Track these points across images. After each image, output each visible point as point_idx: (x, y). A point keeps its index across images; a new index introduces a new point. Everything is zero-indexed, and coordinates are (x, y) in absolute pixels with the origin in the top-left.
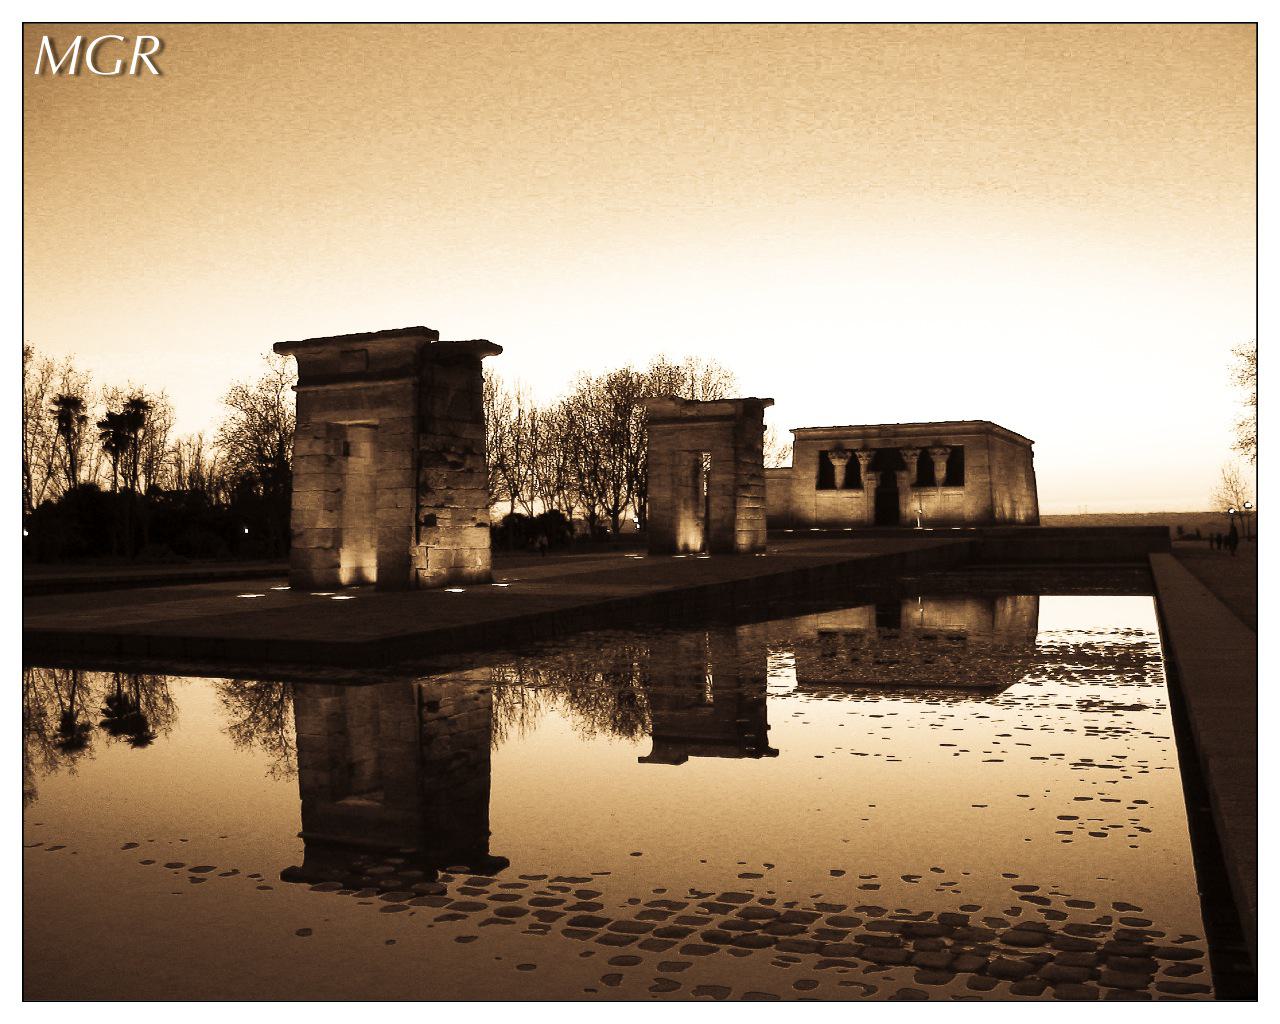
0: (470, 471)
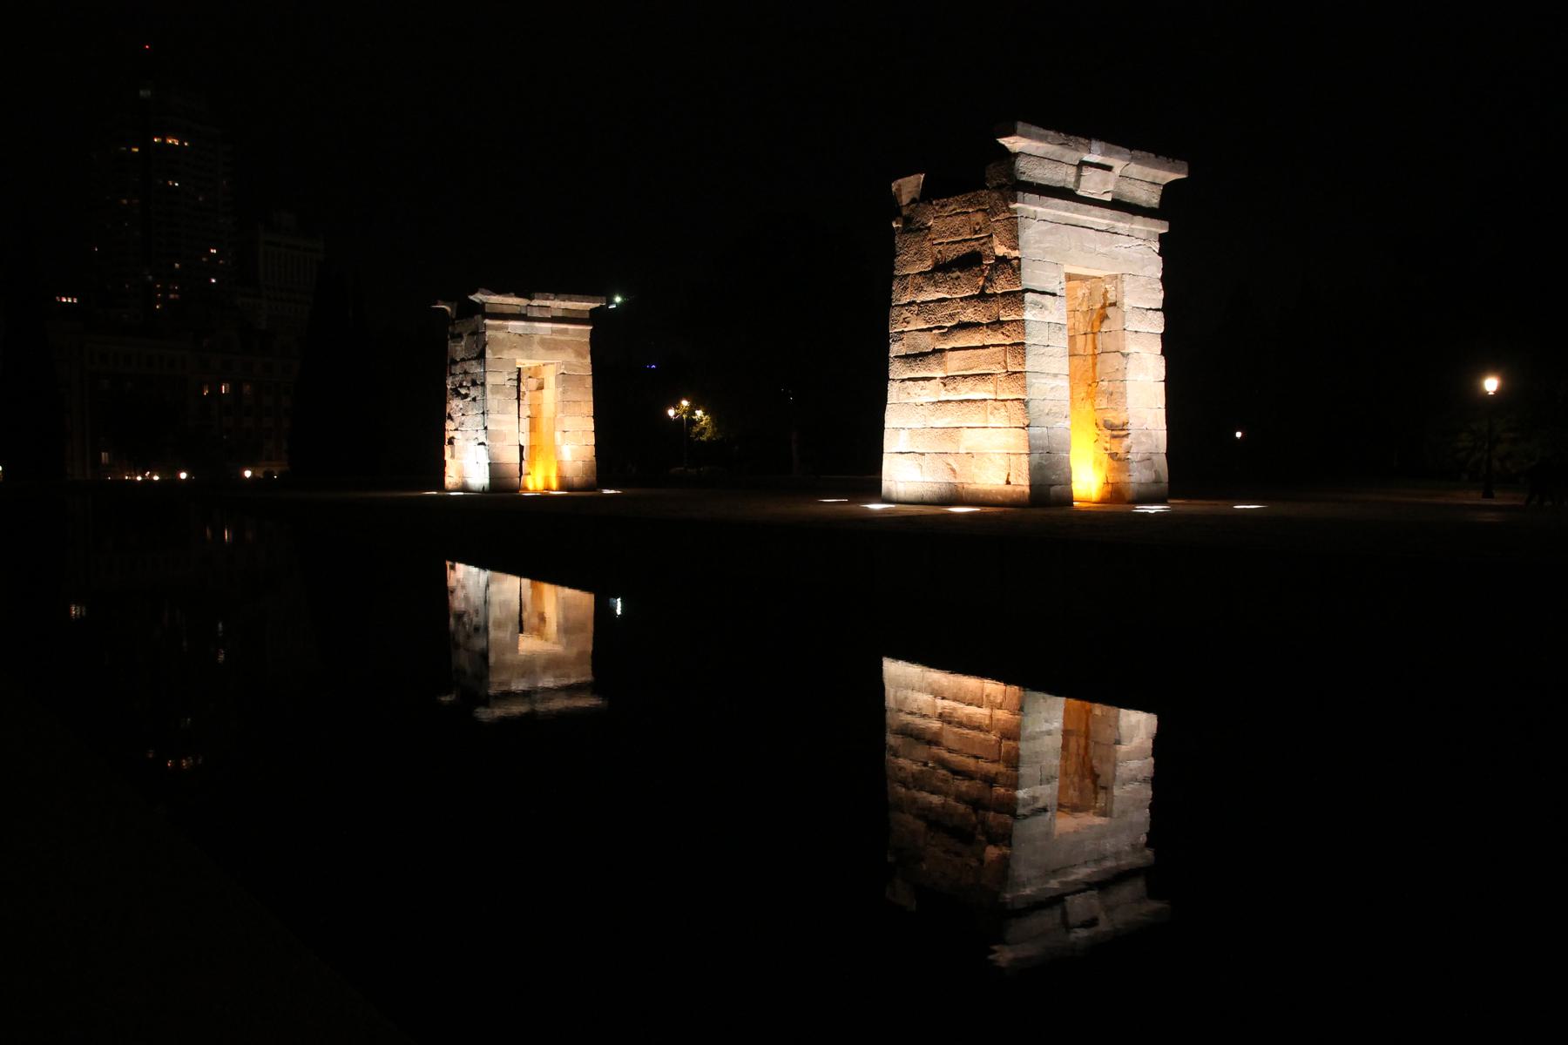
0: (474, 399)
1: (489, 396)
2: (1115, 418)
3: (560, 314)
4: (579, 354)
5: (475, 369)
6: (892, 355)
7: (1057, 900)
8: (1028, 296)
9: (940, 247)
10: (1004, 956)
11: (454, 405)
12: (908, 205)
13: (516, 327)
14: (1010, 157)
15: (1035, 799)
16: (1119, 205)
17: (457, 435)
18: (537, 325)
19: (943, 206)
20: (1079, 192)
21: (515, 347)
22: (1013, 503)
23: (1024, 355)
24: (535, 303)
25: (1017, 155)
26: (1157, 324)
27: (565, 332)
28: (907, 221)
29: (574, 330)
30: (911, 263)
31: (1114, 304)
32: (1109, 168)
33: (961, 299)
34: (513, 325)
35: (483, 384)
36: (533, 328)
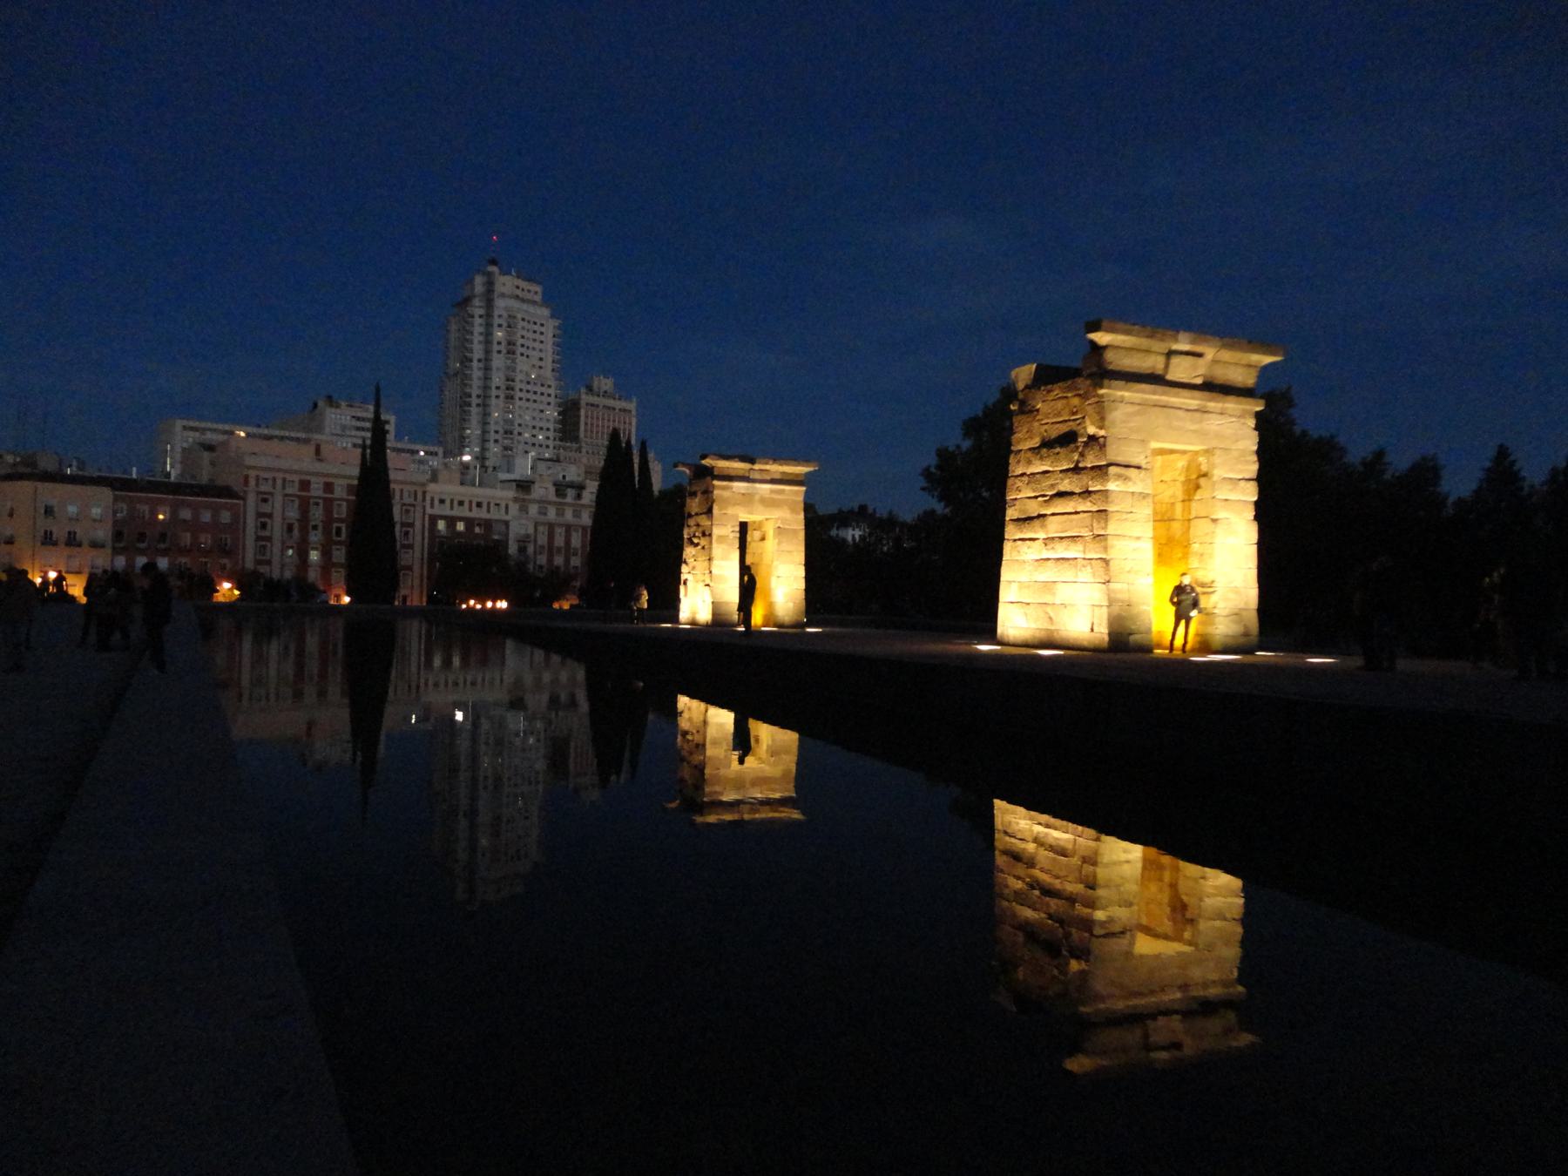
1: (715, 545)
4: (793, 511)
5: (704, 521)
6: (1007, 519)
8: (1112, 470)
9: (1046, 427)
10: (1078, 1064)
11: (689, 552)
12: (1023, 390)
13: (739, 488)
15: (1111, 920)
16: (1211, 387)
17: (689, 577)
18: (758, 485)
19: (1049, 391)
20: (1169, 377)
21: (738, 504)
22: (1096, 650)
23: (1106, 521)
24: (757, 467)
25: (1105, 347)
26: (1251, 493)
27: (782, 492)
28: (1023, 403)
29: (791, 491)
30: (1025, 439)
31: (1205, 475)
32: (1200, 355)
33: (1061, 471)
35: (710, 535)
36: (755, 488)
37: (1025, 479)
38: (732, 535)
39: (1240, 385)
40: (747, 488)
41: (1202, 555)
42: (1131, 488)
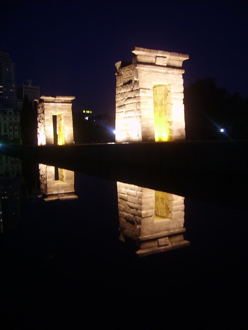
2: (170, 120)
3: (63, 101)
4: (69, 111)
5: (42, 115)
6: (116, 106)
7: (156, 239)
9: (124, 79)
10: (139, 252)
11: (39, 124)
12: (118, 69)
14: (135, 56)
15: (147, 214)
19: (124, 69)
20: (157, 64)
24: (57, 98)
25: (137, 55)
28: (118, 73)
29: (68, 105)
30: (119, 83)
31: (169, 91)
32: (165, 57)
34: (51, 104)
35: (44, 119)
37: (120, 94)
38: (50, 119)
39: (177, 66)
40: (54, 105)
41: (169, 114)
42: (146, 95)
